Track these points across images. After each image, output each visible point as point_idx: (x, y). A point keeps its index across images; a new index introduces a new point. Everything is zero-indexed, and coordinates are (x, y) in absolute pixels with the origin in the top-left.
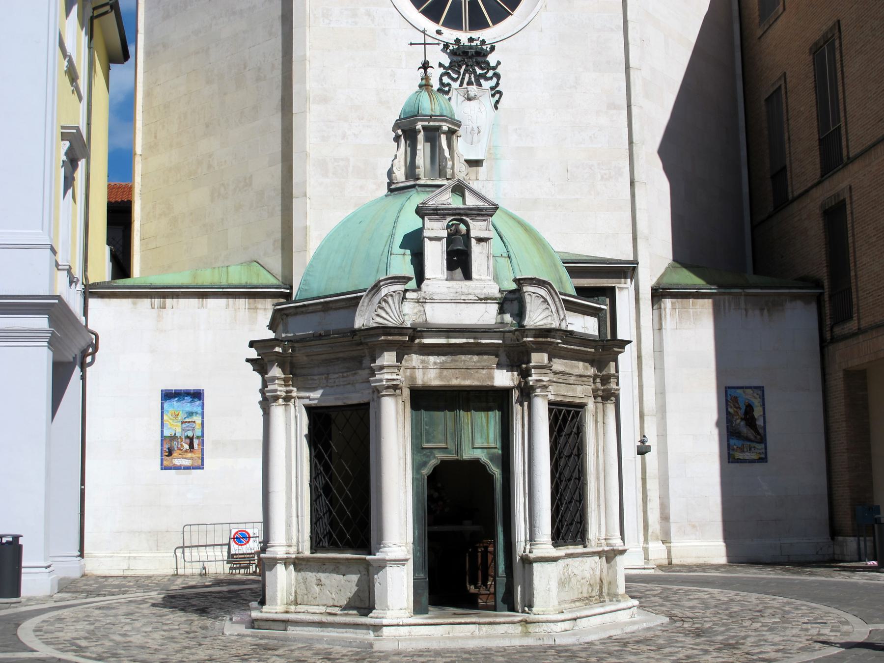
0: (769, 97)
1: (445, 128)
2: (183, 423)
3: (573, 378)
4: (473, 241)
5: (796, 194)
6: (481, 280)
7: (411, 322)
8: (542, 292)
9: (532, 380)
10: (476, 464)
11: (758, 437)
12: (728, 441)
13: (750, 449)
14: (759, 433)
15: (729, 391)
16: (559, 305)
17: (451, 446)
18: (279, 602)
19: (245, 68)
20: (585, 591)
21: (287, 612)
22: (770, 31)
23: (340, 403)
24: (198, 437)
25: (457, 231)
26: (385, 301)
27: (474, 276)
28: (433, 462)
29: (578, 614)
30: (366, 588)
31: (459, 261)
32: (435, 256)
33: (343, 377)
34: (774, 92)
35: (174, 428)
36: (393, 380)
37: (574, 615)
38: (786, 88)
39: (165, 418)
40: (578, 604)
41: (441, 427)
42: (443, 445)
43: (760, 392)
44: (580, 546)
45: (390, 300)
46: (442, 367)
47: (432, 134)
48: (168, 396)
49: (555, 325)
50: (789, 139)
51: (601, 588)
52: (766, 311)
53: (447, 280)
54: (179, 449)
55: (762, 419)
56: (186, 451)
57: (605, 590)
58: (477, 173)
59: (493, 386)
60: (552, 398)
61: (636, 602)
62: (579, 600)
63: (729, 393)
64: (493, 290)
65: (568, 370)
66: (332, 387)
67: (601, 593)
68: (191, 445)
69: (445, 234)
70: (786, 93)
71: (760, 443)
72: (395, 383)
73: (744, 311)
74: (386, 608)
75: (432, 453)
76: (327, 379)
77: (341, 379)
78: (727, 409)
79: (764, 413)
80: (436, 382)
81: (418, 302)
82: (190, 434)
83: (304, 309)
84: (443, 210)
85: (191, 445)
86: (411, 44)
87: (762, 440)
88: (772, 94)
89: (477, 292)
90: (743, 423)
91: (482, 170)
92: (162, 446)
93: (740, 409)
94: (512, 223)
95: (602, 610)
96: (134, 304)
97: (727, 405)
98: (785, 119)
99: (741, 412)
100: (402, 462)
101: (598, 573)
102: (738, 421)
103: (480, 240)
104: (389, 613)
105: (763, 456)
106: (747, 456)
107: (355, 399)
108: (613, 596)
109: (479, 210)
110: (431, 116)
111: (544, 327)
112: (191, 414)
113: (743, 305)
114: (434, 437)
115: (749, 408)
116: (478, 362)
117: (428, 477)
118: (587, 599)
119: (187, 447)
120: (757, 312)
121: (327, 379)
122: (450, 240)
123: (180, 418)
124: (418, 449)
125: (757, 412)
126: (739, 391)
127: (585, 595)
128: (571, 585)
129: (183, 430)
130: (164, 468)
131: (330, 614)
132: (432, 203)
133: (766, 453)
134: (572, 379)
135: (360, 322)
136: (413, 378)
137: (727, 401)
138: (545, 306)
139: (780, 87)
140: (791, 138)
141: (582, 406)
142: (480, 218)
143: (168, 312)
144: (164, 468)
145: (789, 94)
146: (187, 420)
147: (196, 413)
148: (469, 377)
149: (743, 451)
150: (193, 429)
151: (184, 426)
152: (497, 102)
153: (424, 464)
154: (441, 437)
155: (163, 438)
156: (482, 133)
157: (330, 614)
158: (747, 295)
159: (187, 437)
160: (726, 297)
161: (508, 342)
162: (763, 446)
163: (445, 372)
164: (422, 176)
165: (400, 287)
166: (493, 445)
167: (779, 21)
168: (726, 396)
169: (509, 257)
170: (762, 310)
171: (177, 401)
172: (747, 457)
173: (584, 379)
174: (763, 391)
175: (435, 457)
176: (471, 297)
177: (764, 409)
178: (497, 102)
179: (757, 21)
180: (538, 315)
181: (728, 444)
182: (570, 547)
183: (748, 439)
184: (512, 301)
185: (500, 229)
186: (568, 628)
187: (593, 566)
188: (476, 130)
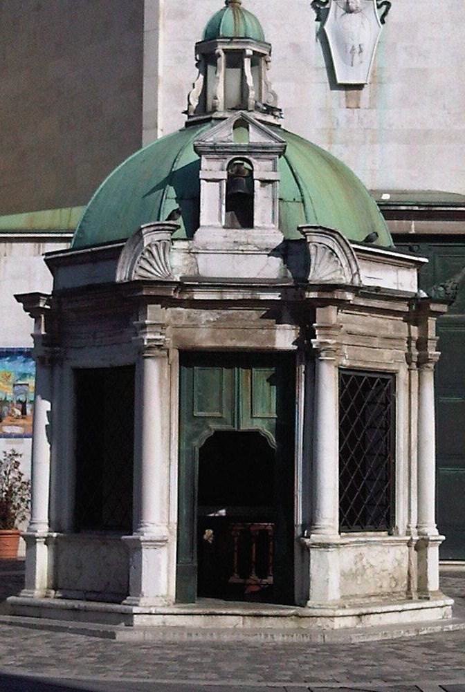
1: (249, 52)
2: (14, 385)
3: (377, 340)
6: (264, 228)
7: (180, 275)
8: (329, 242)
9: (315, 342)
10: (255, 435)
16: (351, 258)
17: (226, 414)
18: (37, 586)
20: (385, 584)
23: (106, 364)
24: (31, 402)
25: (239, 172)
26: (151, 252)
27: (256, 223)
28: (206, 433)
29: (364, 611)
31: (240, 207)
32: (211, 199)
33: (110, 336)
36: (156, 340)
37: (357, 612)
40: (373, 599)
41: (216, 394)
42: (217, 414)
44: (384, 533)
47: (235, 60)
49: (346, 280)
51: (409, 583)
53: (224, 227)
57: (414, 586)
58: (359, 99)
59: (273, 349)
60: (345, 362)
64: (277, 239)
65: (371, 331)
67: (409, 589)
68: (24, 412)
69: (224, 175)
74: (139, 592)
75: (204, 422)
76: (95, 338)
77: (108, 339)
80: (210, 344)
81: (189, 253)
82: (22, 398)
84: (223, 147)
85: (24, 412)
89: (256, 241)
91: (365, 93)
94: (316, 161)
95: (399, 608)
100: (166, 431)
101: (405, 565)
103: (264, 182)
107: (121, 360)
108: (424, 594)
109: (267, 148)
110: (232, 38)
111: (332, 282)
112: (24, 376)
114: (208, 405)
117: (200, 449)
118: (389, 594)
119: (18, 412)
121: (95, 338)
122: (232, 182)
124: (187, 415)
127: (386, 589)
128: (365, 577)
129: (15, 393)
132: (210, 140)
134: (376, 342)
135: (121, 275)
141: (394, 374)
142: (266, 156)
146: (19, 382)
147: (30, 375)
148: (246, 338)
150: (26, 393)
151: (16, 388)
152: (385, 14)
154: (215, 405)
156: (364, 53)
159: (19, 402)
161: (290, 299)
163: (219, 333)
164: (221, 107)
169: (303, 201)
175: (208, 428)
176: (250, 247)
178: (385, 14)
180: (322, 271)
184: (293, 252)
185: (297, 169)
187: (398, 557)
188: (358, 50)
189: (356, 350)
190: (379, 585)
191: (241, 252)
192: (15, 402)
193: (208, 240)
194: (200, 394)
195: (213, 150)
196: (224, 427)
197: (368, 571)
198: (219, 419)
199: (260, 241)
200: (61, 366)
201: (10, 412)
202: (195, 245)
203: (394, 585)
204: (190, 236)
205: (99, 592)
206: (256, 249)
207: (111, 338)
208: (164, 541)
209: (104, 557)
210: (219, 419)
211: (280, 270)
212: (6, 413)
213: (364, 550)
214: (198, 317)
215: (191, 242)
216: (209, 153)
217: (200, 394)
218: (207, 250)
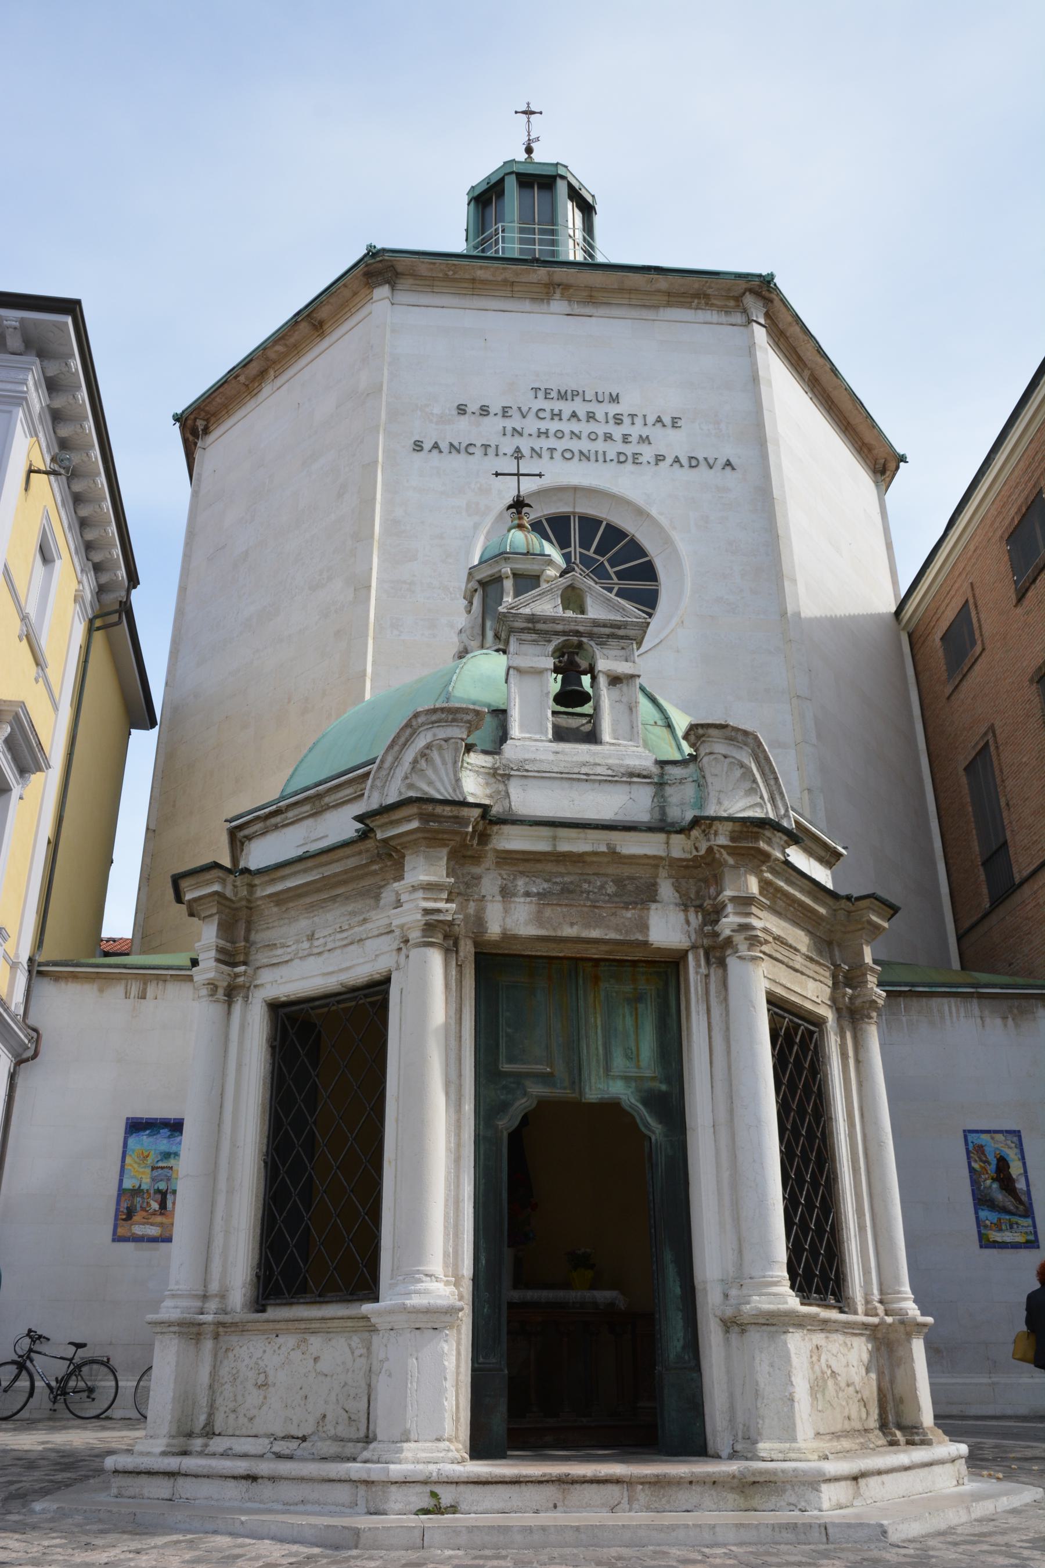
0: (971, 763)
2: (153, 1168)
4: (602, 681)
5: (1026, 873)
9: (730, 920)
10: (612, 1108)
11: (1021, 1207)
12: (976, 1213)
13: (1011, 1228)
14: (1021, 1202)
15: (970, 1137)
19: (289, 702)
20: (854, 1415)
21: (185, 1453)
22: (964, 683)
28: (521, 1105)
30: (364, 1386)
34: (978, 754)
35: (140, 1176)
36: (438, 911)
38: (996, 742)
39: (128, 1160)
43: (1015, 1139)
45: (435, 755)
48: (136, 1126)
50: (1008, 804)
52: (1010, 1021)
54: (143, 1209)
55: (1023, 1180)
56: (154, 1213)
59: (646, 944)
61: (963, 1449)
62: (846, 1434)
63: (970, 1139)
66: (320, 954)
70: (997, 748)
71: (1026, 1216)
72: (441, 917)
73: (979, 1020)
78: (969, 1164)
79: (1026, 1171)
80: (532, 931)
82: (162, 1186)
83: (277, 819)
85: (163, 1205)
86: (497, 474)
87: (1028, 1212)
88: (975, 758)
89: (610, 761)
90: (995, 1186)
92: (118, 1203)
93: (989, 1164)
96: (101, 990)
97: (969, 1157)
98: (998, 780)
99: (992, 1168)
102: (989, 1182)
103: (615, 680)
104: (409, 1449)
105: (1032, 1238)
106: (1007, 1237)
113: (977, 1012)
115: (1003, 1164)
116: (615, 895)
117: (510, 1135)
119: (155, 1206)
120: (998, 1022)
123: (149, 1161)
125: (1016, 1169)
126: (983, 1136)
129: (154, 1180)
130: (117, 1238)
131: (279, 1456)
133: (1036, 1233)
136: (479, 921)
137: (968, 1152)
138: (748, 785)
139: (987, 742)
140: (1011, 803)
143: (149, 1004)
144: (117, 1238)
145: (1001, 748)
146: (160, 1164)
149: (1001, 1230)
151: (156, 1173)
153: (503, 1107)
155: (121, 1192)
157: (279, 1456)
158: (981, 996)
160: (952, 1000)
161: (677, 853)
162: (1029, 1221)
163: (548, 912)
165: (457, 732)
166: (648, 1073)
167: (977, 667)
168: (966, 1143)
170: (1005, 1018)
171: (149, 1135)
172: (1008, 1240)
174: (1020, 1137)
175: (525, 1094)
176: (599, 770)
177: (1024, 1164)
179: (945, 675)
181: (977, 1218)
183: (1005, 1210)
186: (843, 1501)
191: (585, 777)
192: (152, 1192)
193: (527, 756)
194: (509, 1030)
195: (530, 625)
196: (559, 1092)
198: (546, 1079)
199: (617, 762)
200: (246, 998)
201: (145, 1205)
202: (504, 762)
204: (495, 750)
205: (304, 1439)
206: (610, 772)
207: (344, 935)
208: (451, 1311)
209: (316, 1359)
210: (546, 1079)
211: (652, 809)
212: (138, 1206)
214: (510, 885)
215: (497, 757)
216: (522, 630)
217: (509, 1030)
218: (527, 771)
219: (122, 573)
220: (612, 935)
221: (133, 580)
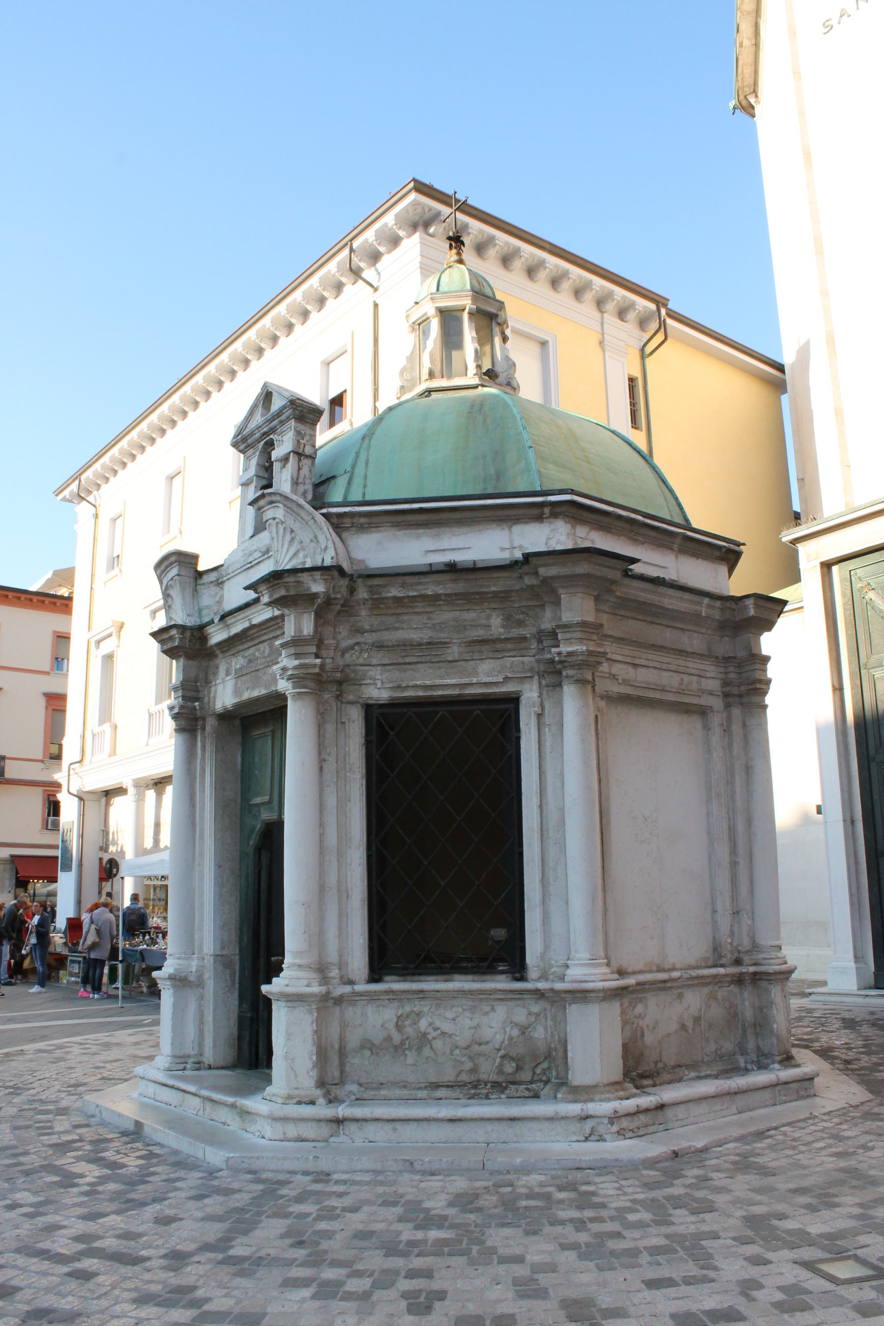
37: (329, 1112)
40: (441, 1093)
46: (240, 674)
116: (269, 655)
128: (427, 1051)
134: (454, 651)
173: (499, 646)
182: (457, 977)
189: (405, 671)
190: (469, 1065)
197: (438, 1044)
203: (510, 1068)
213: (424, 1006)
219: (642, 304)
220: (264, 692)
221: (660, 302)
